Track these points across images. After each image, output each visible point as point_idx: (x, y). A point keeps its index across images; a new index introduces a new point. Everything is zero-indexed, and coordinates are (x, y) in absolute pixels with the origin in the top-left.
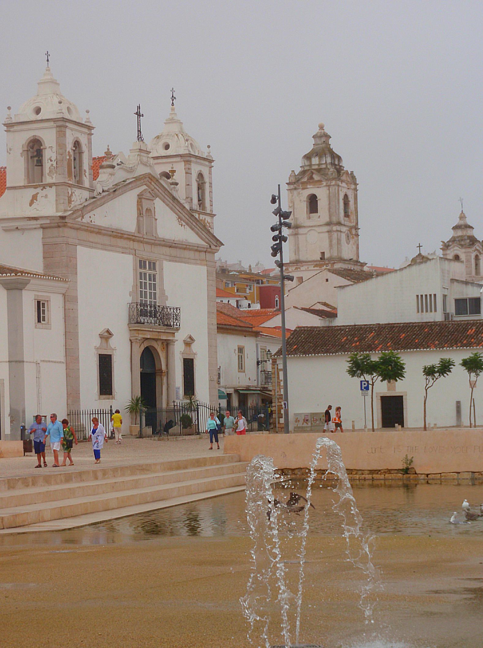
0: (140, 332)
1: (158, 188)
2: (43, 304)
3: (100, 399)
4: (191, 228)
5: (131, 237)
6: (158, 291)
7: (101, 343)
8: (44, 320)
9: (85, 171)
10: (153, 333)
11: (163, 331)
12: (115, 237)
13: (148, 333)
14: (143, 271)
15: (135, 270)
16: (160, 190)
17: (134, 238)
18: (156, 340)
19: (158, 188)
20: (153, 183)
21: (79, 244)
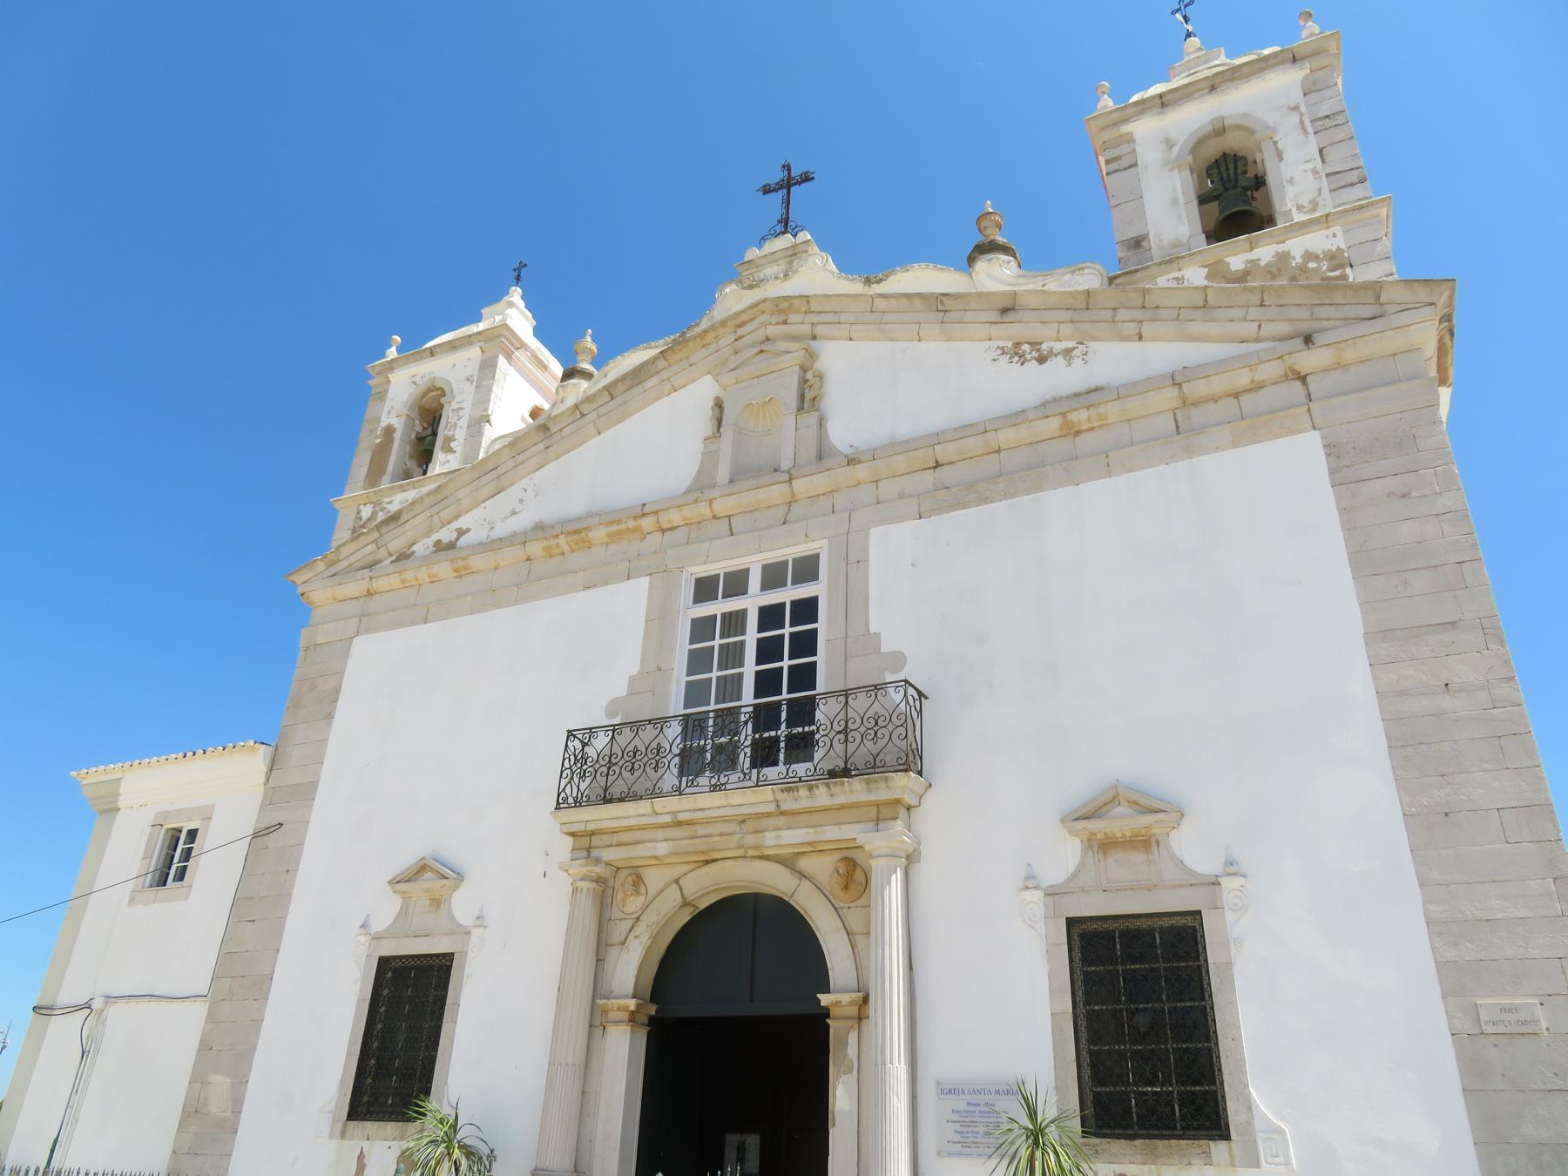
0: (596, 841)
1: (830, 318)
2: (193, 834)
3: (343, 1135)
4: (1124, 338)
5: (631, 524)
6: (820, 658)
7: (404, 912)
8: (181, 876)
9: (451, 439)
10: (701, 831)
11: (771, 808)
12: (571, 549)
13: (660, 834)
14: (719, 607)
15: (658, 618)
16: (844, 318)
17: (647, 523)
18: (787, 862)
19: (830, 318)
20: (792, 318)
21: (368, 631)
